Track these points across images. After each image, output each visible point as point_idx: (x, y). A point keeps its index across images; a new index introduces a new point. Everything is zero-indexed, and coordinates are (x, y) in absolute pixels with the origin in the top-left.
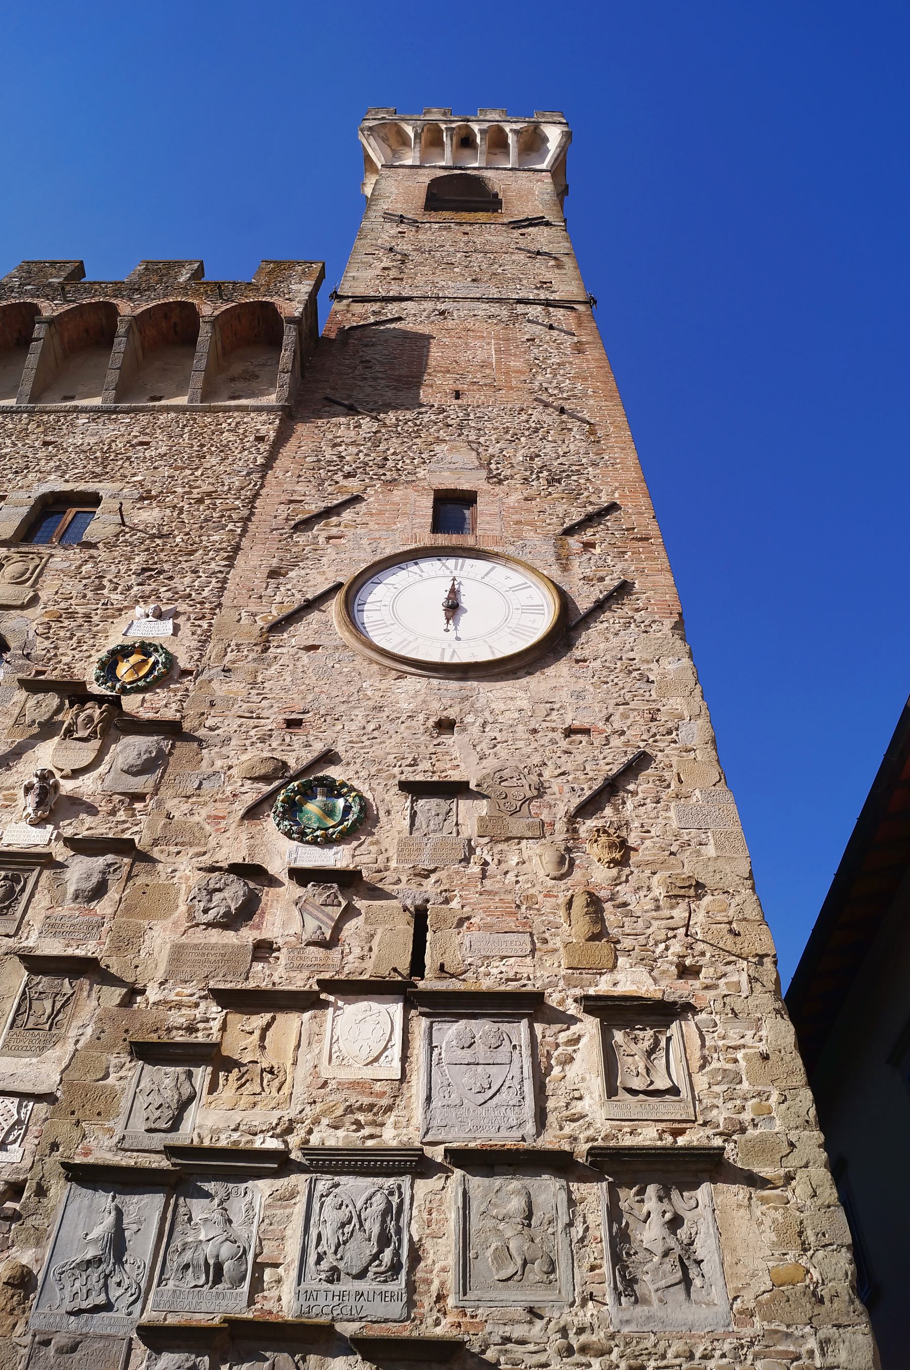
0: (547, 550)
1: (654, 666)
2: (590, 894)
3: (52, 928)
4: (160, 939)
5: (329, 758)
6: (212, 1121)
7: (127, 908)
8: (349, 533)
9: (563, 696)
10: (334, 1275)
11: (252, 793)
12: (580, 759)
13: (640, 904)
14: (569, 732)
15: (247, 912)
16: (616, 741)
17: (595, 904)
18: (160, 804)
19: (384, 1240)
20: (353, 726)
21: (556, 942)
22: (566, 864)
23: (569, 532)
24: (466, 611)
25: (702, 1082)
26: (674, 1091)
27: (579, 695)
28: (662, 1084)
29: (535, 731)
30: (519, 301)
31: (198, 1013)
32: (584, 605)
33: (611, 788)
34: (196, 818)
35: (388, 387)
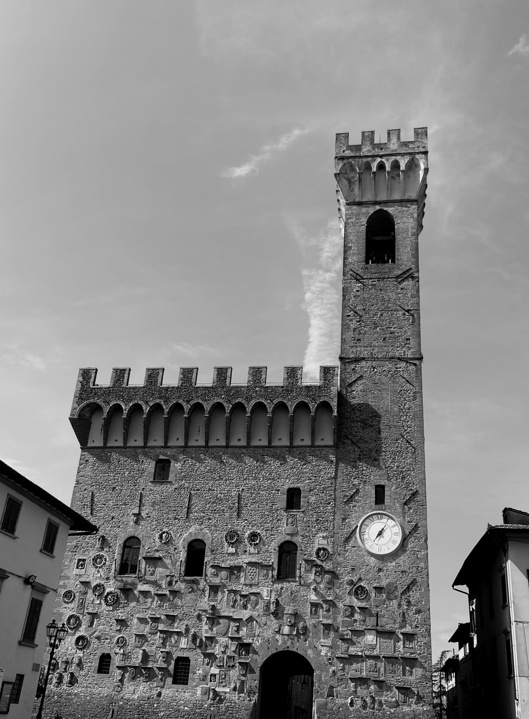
0: (400, 510)
1: (419, 553)
2: (403, 612)
3: (324, 617)
4: (340, 619)
5: (360, 579)
6: (353, 650)
7: (334, 613)
8: (357, 504)
9: (401, 562)
10: (370, 672)
11: (349, 588)
12: (404, 579)
13: (411, 614)
14: (402, 572)
15: (352, 615)
16: (410, 575)
17: (404, 613)
18: (334, 590)
19: (376, 667)
20: (364, 570)
21: (398, 621)
22: (400, 605)
23: (405, 504)
24: (383, 537)
25: (416, 646)
26: (412, 648)
27: (404, 562)
28: (411, 646)
29: (396, 572)
30: (399, 359)
31: (347, 632)
32: (407, 532)
33: (408, 589)
34: (340, 593)
35: (361, 426)
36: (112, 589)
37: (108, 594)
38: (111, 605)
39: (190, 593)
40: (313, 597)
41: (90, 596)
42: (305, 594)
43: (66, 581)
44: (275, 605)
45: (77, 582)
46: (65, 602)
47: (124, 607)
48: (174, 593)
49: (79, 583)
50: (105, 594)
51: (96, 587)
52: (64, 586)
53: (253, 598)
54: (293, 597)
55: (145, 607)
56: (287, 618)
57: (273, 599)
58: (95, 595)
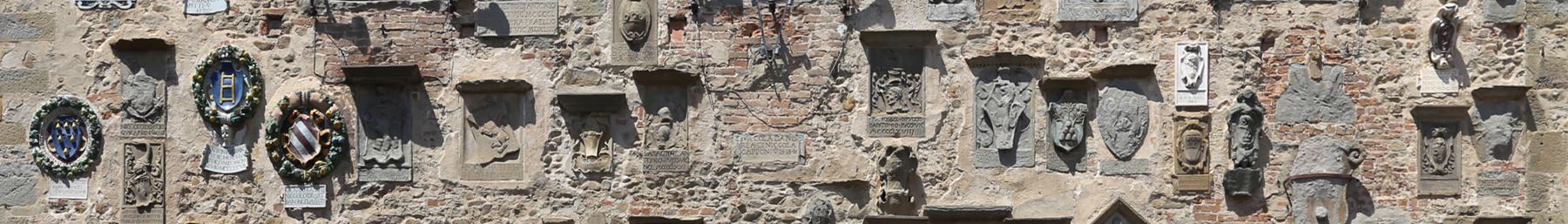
36: (307, 85)
37: (289, 113)
38: (316, 180)
39: (756, 86)
40: (1429, 84)
41: (184, 128)
42: (1390, 67)
43: (40, 48)
44: (1242, 135)
45: (104, 52)
46: (49, 171)
47: (390, 186)
48: (673, 90)
49: (110, 57)
50: (272, 110)
51: (209, 74)
52: (30, 76)
53: (1112, 98)
54: (1328, 85)
55: (512, 184)
56: (1311, 201)
57: (1225, 102)
58: (214, 123)
